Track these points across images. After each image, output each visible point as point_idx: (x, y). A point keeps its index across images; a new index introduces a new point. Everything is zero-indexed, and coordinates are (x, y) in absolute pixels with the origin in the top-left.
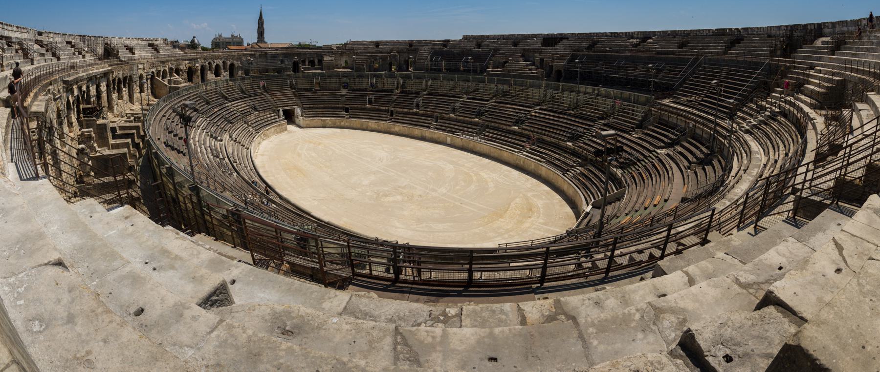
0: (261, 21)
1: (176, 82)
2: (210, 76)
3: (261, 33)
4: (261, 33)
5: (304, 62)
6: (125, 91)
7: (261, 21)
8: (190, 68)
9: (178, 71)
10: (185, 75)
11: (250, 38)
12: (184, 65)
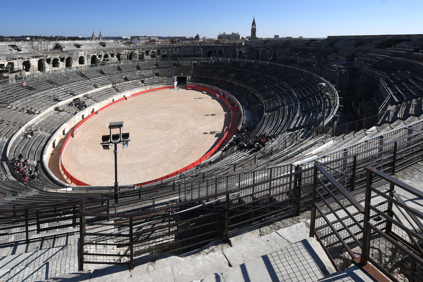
12: (124, 53)
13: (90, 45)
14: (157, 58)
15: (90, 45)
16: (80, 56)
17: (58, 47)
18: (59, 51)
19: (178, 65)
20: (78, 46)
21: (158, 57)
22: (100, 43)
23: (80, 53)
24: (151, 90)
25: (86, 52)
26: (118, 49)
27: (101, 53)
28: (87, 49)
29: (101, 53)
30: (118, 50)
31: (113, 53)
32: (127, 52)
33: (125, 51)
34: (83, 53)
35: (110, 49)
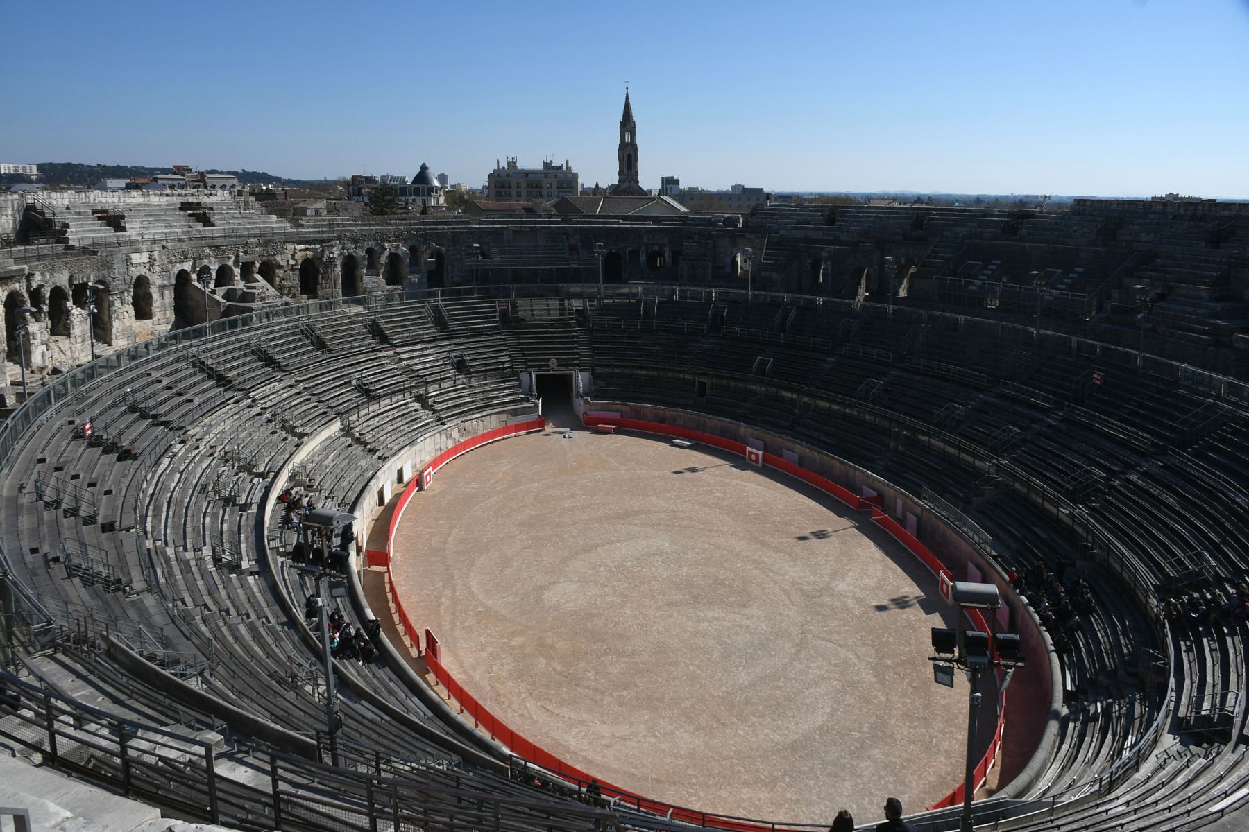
0: (627, 125)
1: (247, 297)
2: (374, 283)
3: (628, 156)
4: (628, 156)
5: (635, 254)
6: (79, 318)
7: (627, 125)
8: (307, 263)
9: (268, 271)
10: (294, 279)
11: (597, 171)
12: (291, 255)
13: (154, 215)
14: (411, 283)
15: (154, 215)
16: (135, 272)
17: (35, 226)
18: (46, 247)
19: (509, 320)
20: (113, 220)
21: (415, 278)
22: (184, 206)
23: (136, 258)
24: (473, 441)
25: (156, 254)
26: (270, 241)
27: (208, 257)
28: (152, 235)
29: (208, 257)
30: (267, 243)
31: (248, 258)
32: (298, 255)
33: (291, 247)
34: (144, 258)
35: (240, 241)
